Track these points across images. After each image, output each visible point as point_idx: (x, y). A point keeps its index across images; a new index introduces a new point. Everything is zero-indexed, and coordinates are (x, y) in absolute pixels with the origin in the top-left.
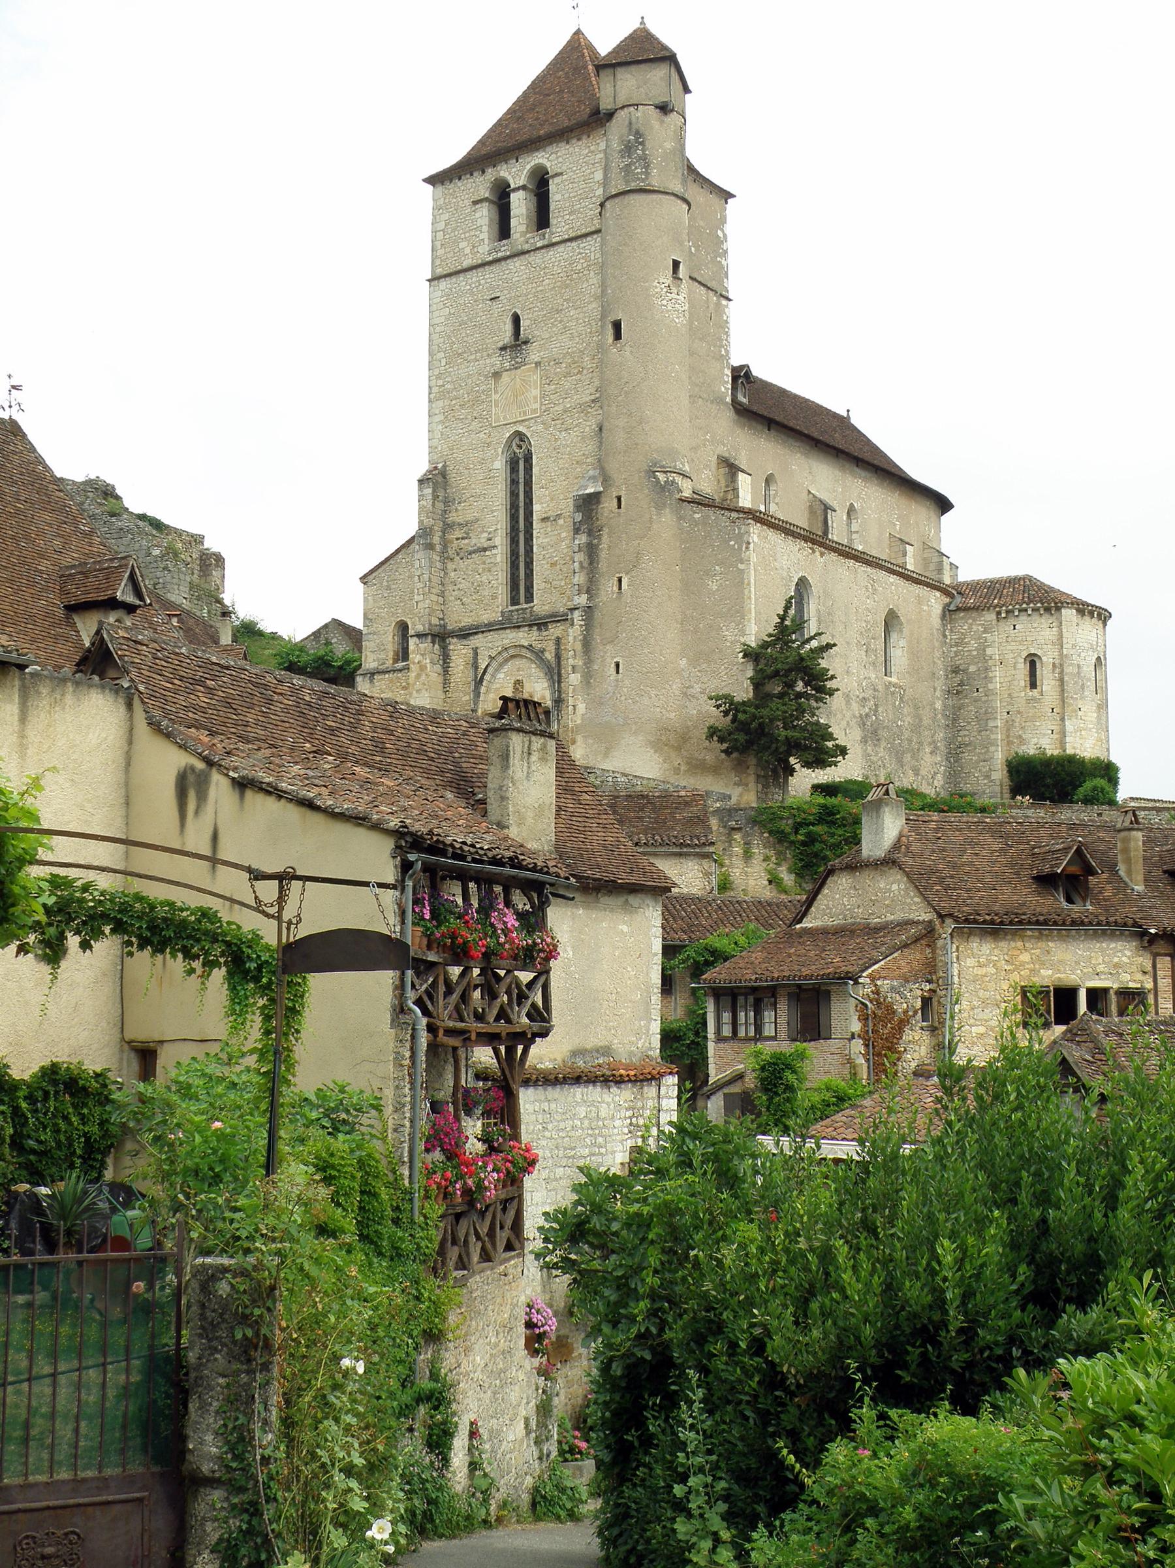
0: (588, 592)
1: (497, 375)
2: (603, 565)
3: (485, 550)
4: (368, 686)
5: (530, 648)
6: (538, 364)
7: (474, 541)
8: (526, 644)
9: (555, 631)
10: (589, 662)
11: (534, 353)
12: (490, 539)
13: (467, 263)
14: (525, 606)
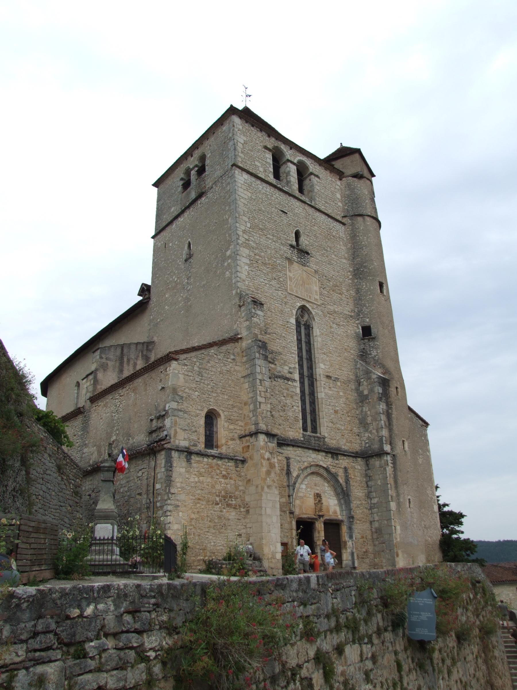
0: (391, 444)
3: (288, 379)
4: (184, 464)
5: (327, 469)
6: (316, 272)
8: (325, 466)
10: (398, 495)
12: (290, 373)
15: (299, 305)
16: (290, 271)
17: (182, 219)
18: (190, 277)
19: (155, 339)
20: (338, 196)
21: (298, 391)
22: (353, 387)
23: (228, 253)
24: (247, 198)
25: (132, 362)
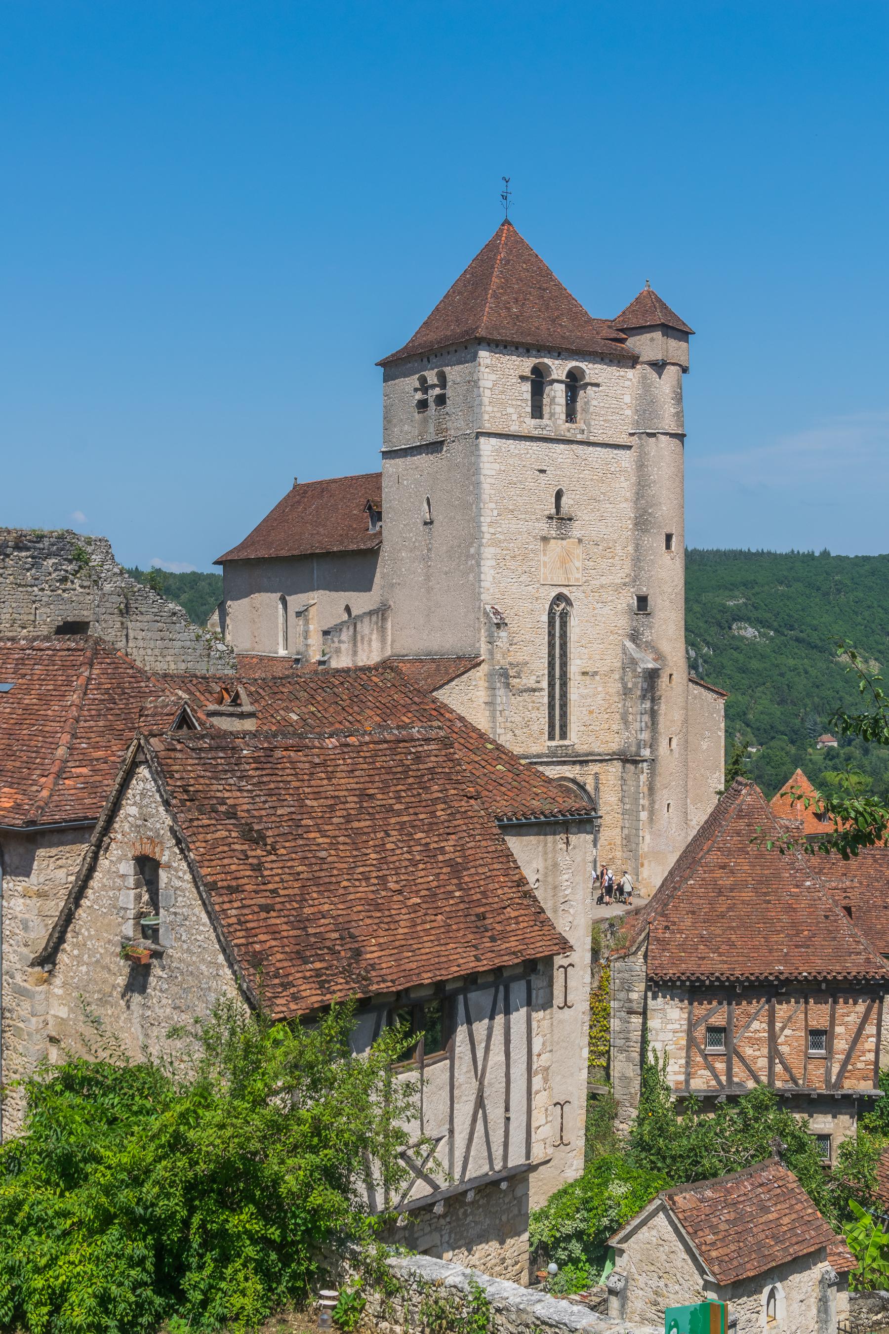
0: (651, 747)
1: (545, 539)
2: (661, 727)
3: (534, 690)
6: (580, 541)
7: (524, 681)
8: (571, 776)
9: (594, 768)
10: (652, 802)
11: (576, 530)
12: (538, 682)
13: (514, 428)
14: (562, 743)
15: (553, 594)
16: (545, 555)
19: (391, 603)
20: (627, 399)
21: (546, 700)
22: (617, 677)
23: (472, 550)
24: (493, 473)
25: (366, 639)
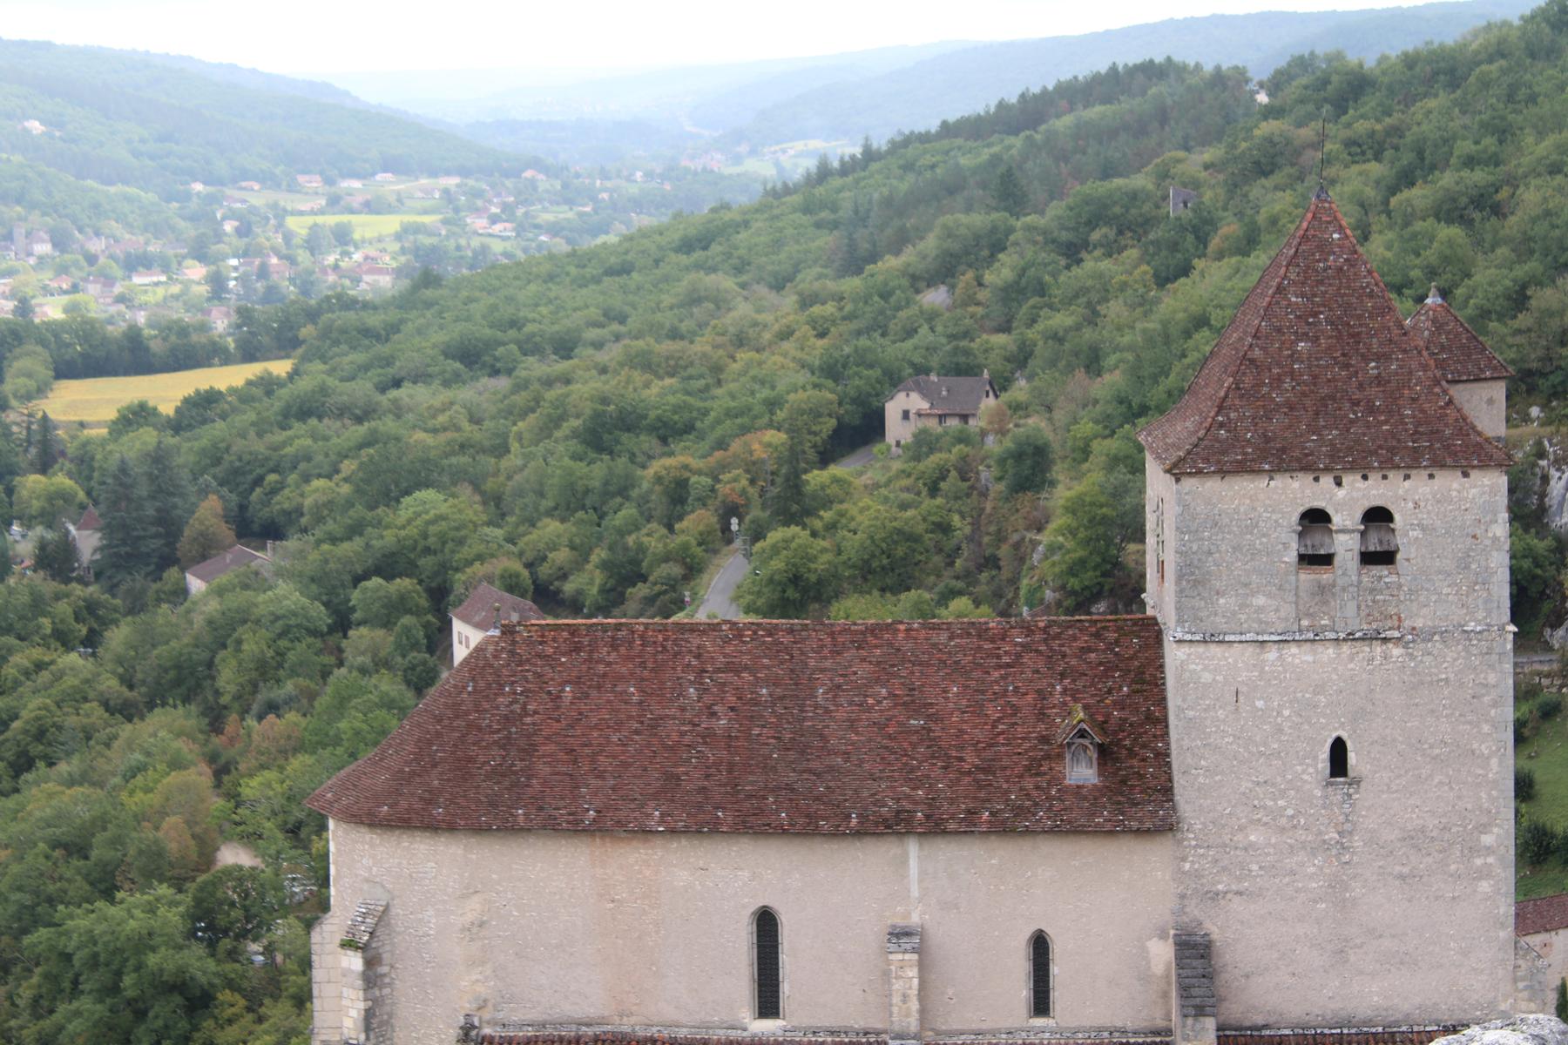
17: (1310, 658)
18: (1351, 833)
23: (1487, 840)
